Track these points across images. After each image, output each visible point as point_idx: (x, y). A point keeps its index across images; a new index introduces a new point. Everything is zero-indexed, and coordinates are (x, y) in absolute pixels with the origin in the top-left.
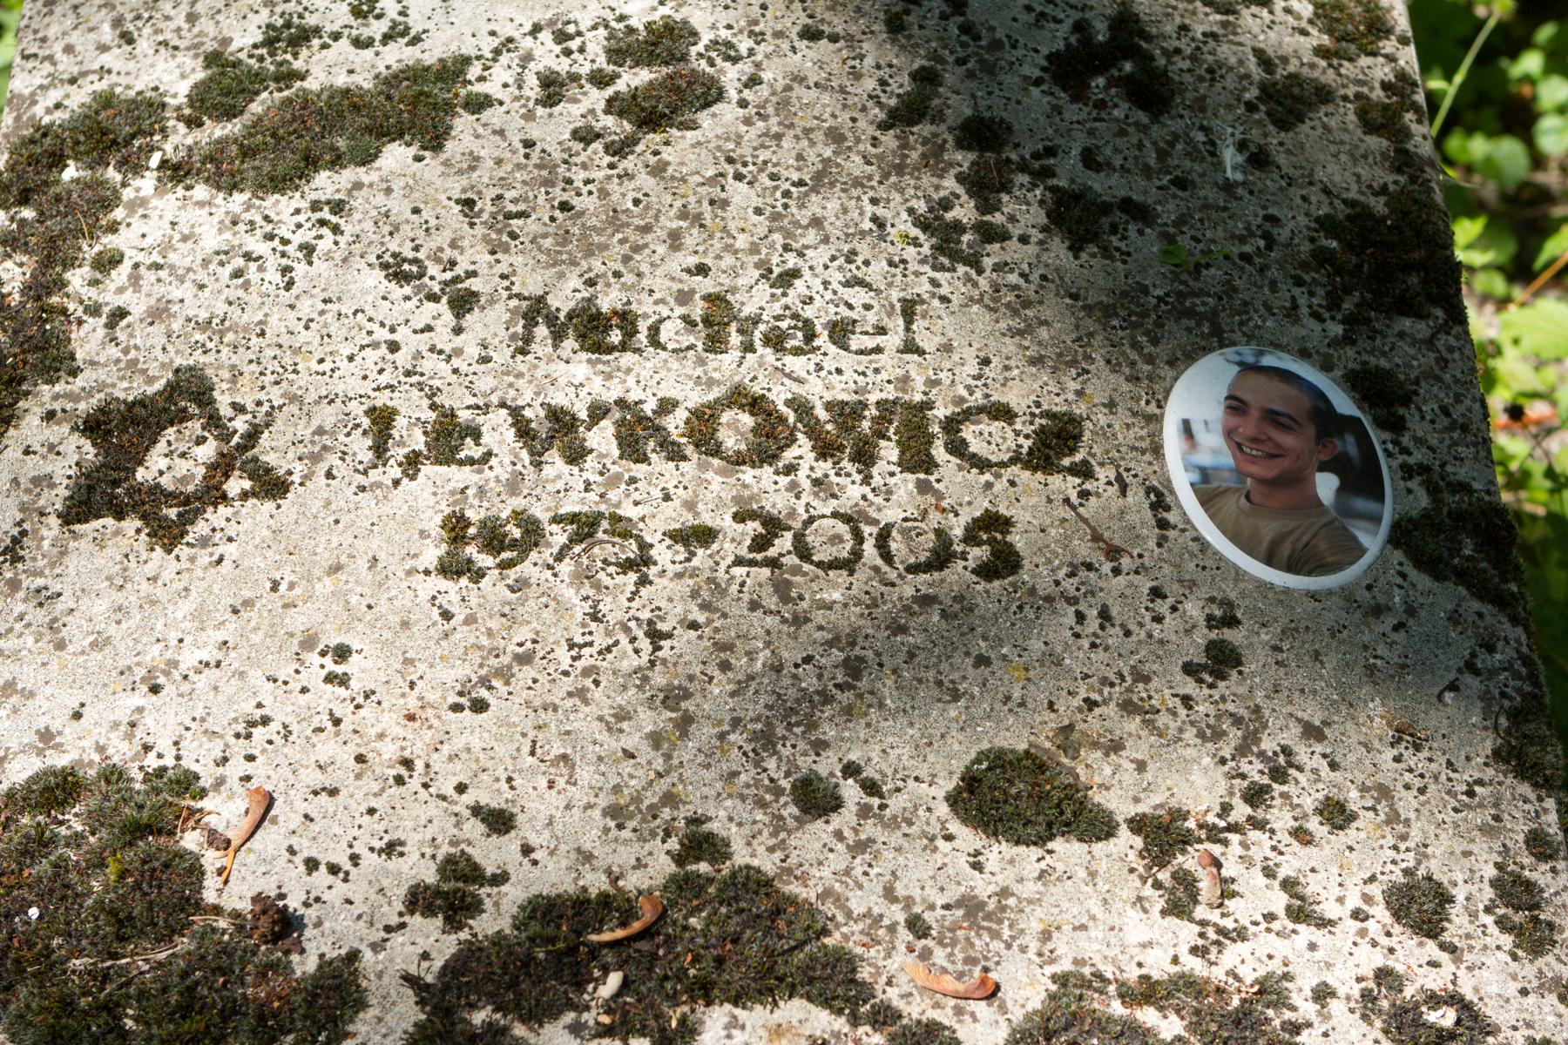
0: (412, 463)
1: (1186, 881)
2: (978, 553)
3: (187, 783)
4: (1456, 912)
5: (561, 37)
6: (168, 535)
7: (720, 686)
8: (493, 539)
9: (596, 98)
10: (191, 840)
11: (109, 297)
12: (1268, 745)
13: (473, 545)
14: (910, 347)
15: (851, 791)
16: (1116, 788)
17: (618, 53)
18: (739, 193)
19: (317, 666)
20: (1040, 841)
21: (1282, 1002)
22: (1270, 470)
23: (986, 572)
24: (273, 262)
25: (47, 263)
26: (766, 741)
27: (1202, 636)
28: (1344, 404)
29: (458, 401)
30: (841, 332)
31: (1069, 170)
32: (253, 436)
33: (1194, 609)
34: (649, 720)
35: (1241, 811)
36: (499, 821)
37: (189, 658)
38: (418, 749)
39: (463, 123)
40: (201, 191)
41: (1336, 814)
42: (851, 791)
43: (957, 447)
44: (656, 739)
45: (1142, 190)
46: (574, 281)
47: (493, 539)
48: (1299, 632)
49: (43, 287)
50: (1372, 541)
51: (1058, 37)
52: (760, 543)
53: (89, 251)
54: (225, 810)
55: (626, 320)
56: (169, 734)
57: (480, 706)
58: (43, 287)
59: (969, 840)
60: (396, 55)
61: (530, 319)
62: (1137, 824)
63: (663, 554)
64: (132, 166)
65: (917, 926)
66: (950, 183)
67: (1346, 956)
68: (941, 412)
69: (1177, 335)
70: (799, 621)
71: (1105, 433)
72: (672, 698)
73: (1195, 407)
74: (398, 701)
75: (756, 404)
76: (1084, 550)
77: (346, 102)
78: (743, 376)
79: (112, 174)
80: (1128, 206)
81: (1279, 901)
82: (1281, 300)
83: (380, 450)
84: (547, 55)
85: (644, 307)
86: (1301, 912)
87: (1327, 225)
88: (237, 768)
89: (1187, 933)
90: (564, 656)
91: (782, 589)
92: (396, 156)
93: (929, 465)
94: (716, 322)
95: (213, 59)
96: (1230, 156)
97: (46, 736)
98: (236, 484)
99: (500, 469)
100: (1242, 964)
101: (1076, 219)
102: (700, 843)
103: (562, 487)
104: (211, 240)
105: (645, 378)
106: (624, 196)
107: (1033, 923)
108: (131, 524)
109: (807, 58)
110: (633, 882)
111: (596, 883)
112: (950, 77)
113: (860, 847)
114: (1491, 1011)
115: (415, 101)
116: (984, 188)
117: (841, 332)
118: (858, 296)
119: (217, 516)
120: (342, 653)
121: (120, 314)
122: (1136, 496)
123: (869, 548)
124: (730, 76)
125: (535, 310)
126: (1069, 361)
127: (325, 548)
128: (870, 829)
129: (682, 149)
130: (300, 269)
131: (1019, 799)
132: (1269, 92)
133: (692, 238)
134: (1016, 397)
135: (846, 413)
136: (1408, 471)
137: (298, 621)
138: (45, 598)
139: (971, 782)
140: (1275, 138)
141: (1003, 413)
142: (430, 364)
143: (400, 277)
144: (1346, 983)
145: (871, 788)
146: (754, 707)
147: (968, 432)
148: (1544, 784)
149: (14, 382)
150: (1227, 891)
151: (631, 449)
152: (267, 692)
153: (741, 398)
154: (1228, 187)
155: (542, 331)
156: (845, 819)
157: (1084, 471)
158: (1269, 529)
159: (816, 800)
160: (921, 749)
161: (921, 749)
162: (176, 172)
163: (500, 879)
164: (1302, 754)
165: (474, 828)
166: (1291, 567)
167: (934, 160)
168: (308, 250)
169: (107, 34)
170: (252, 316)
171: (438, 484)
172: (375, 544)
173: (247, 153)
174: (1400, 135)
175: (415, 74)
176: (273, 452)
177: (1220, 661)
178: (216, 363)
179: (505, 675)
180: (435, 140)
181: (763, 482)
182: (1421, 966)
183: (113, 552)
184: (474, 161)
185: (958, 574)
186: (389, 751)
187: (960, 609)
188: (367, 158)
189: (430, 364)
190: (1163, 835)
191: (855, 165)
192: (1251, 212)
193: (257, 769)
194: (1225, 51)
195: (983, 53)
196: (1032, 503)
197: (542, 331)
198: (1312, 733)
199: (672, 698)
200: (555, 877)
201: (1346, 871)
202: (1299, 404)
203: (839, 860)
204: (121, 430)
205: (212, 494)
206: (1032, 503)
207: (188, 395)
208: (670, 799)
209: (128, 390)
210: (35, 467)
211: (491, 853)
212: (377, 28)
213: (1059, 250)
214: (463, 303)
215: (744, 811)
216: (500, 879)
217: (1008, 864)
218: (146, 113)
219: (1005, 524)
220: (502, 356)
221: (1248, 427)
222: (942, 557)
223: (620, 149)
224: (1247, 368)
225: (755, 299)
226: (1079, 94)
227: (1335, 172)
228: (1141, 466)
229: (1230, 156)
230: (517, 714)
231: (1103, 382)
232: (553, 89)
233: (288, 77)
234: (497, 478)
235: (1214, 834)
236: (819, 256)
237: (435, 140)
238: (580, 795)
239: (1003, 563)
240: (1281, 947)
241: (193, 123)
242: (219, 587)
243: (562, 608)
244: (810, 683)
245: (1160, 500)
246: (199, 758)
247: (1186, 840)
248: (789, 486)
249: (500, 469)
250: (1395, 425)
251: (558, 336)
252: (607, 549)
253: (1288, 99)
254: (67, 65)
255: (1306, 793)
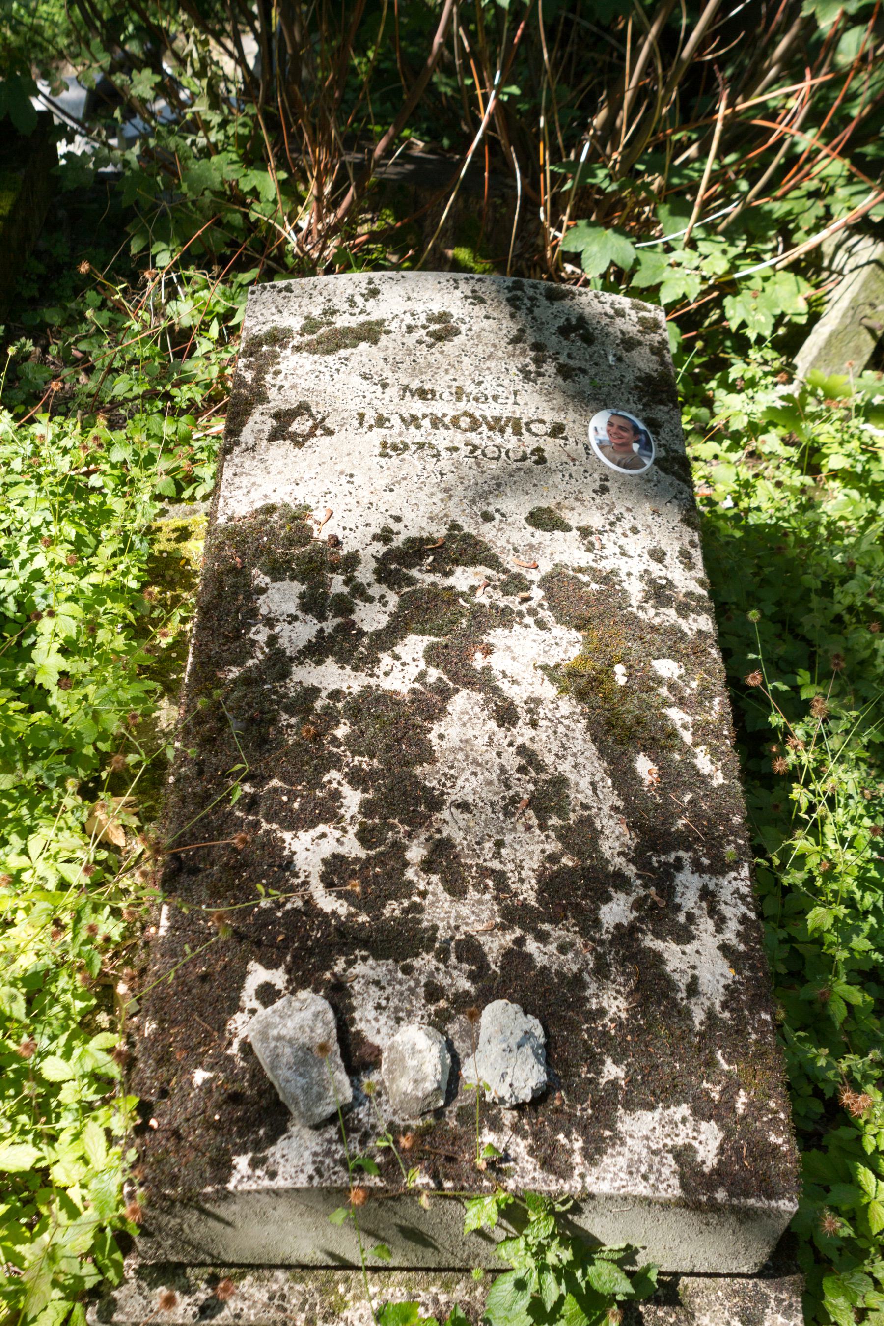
0: (371, 427)
1: (592, 543)
2: (534, 458)
3: (307, 508)
4: (667, 558)
5: (413, 315)
6: (299, 445)
7: (461, 488)
8: (395, 448)
9: (423, 332)
10: (309, 522)
11: (279, 381)
12: (616, 512)
13: (388, 449)
14: (515, 403)
15: (497, 516)
16: (572, 519)
17: (431, 319)
18: (466, 360)
19: (344, 479)
20: (551, 531)
21: (617, 575)
22: (620, 442)
23: (536, 462)
24: (328, 374)
25: (259, 373)
26: (473, 502)
27: (598, 483)
28: (642, 426)
29: (384, 412)
30: (495, 398)
31: (563, 359)
32: (323, 419)
33: (596, 476)
34: (440, 495)
35: (608, 528)
36: (398, 519)
37: (306, 477)
38: (374, 500)
39: (383, 337)
40: (305, 354)
41: (635, 530)
42: (497, 516)
43: (529, 430)
44: (442, 500)
45: (584, 365)
46: (417, 381)
47: (395, 448)
48: (625, 485)
49: (258, 379)
50: (648, 463)
51: (561, 322)
52: (472, 452)
53: (271, 370)
54: (320, 514)
55: (433, 392)
56: (301, 495)
57: (392, 490)
58: (258, 379)
59: (530, 529)
60: (363, 318)
61: (404, 391)
62: (578, 529)
63: (444, 454)
64: (284, 346)
65: (516, 550)
66: (528, 360)
67: (637, 566)
68: (524, 420)
69: (593, 405)
70: (483, 472)
71: (572, 429)
72: (446, 490)
73: (599, 424)
74: (367, 489)
75: (471, 416)
76: (565, 459)
77: (347, 331)
78: (467, 408)
79: (278, 349)
80: (580, 369)
81: (618, 551)
82: (625, 397)
83: (361, 424)
84: (408, 320)
85: (438, 390)
86: (623, 554)
87: (639, 379)
88: (322, 504)
89: (591, 556)
90: (416, 479)
91: (478, 464)
92: (363, 346)
93: (521, 434)
94: (459, 394)
95: (307, 318)
96: (611, 358)
97: (266, 496)
98: (319, 432)
99: (396, 430)
100: (606, 566)
101: (564, 372)
102: (454, 526)
103: (413, 435)
104: (309, 367)
105: (437, 408)
106: (431, 359)
107: (548, 551)
108: (288, 442)
109: (486, 323)
110: (436, 536)
111: (425, 535)
112: (529, 331)
113: (500, 530)
114: (676, 583)
115: (370, 330)
116: (538, 362)
117: (495, 398)
118: (501, 389)
119: (313, 440)
120: (351, 476)
121: (282, 387)
122: (580, 446)
123: (503, 455)
124: (463, 328)
125: (406, 389)
126: (562, 409)
127: (346, 448)
128: (503, 525)
129: (448, 346)
130: (336, 376)
131: (542, 519)
132: (623, 341)
133: (452, 371)
134: (546, 418)
135: (497, 420)
136: (660, 446)
137: (338, 468)
138: (262, 461)
139: (532, 514)
140: (625, 354)
141: (542, 422)
142: (375, 402)
143: (366, 378)
144: (636, 573)
145: (503, 515)
146: (470, 493)
147: (532, 426)
148: (695, 528)
149: (251, 404)
150: (603, 547)
151: (434, 425)
152: (330, 485)
153: (466, 414)
154: (610, 366)
155: (408, 394)
156: (496, 523)
157: (566, 438)
158: (618, 457)
159: (487, 517)
160: (518, 506)
161: (518, 506)
162: (298, 349)
163: (398, 533)
164: (626, 515)
165: (391, 521)
166: (625, 467)
167: (523, 353)
168: (338, 370)
169: (274, 310)
170: (321, 388)
171: (378, 435)
172: (360, 448)
173: (319, 343)
174: (662, 356)
175: (369, 323)
176: (328, 423)
177: (604, 490)
178: (311, 400)
179: (399, 483)
180: (375, 342)
181: (473, 437)
182: (656, 569)
183: (283, 449)
184: (387, 348)
185: (528, 463)
186: (366, 501)
187: (529, 471)
188: (355, 346)
189: (375, 402)
190: (585, 532)
191: (500, 354)
192: (617, 374)
193: (328, 505)
194: (610, 329)
195: (539, 326)
196: (550, 446)
197: (408, 394)
198: (629, 510)
199: (446, 490)
200: (414, 533)
201: (638, 545)
202: (628, 426)
203: (494, 532)
204: (284, 418)
205: (311, 434)
206: (550, 446)
207: (303, 409)
208: (446, 515)
209: (285, 407)
210: (258, 427)
211: (395, 527)
212: (357, 311)
213: (560, 380)
214: (385, 386)
215: (468, 519)
216: (398, 533)
217: (541, 536)
218: (287, 333)
219: (543, 450)
220: (396, 400)
221: (614, 430)
222: (524, 458)
223: (431, 346)
224: (614, 415)
225: (470, 388)
226: (567, 338)
227: (642, 365)
228: (582, 438)
229: (611, 358)
230: (402, 492)
231: (571, 416)
232: (410, 329)
233: (330, 323)
234: (395, 432)
235: (600, 533)
236: (489, 378)
237: (375, 342)
238: (421, 513)
239: (542, 461)
240: (618, 562)
241: (302, 335)
242: (315, 459)
243: (415, 466)
244: (486, 488)
245: (587, 448)
246: (311, 502)
247: (592, 533)
248: (482, 437)
249: (396, 430)
250: (656, 433)
251: (413, 395)
252: (427, 451)
253: (629, 343)
254: (262, 319)
255: (626, 524)
